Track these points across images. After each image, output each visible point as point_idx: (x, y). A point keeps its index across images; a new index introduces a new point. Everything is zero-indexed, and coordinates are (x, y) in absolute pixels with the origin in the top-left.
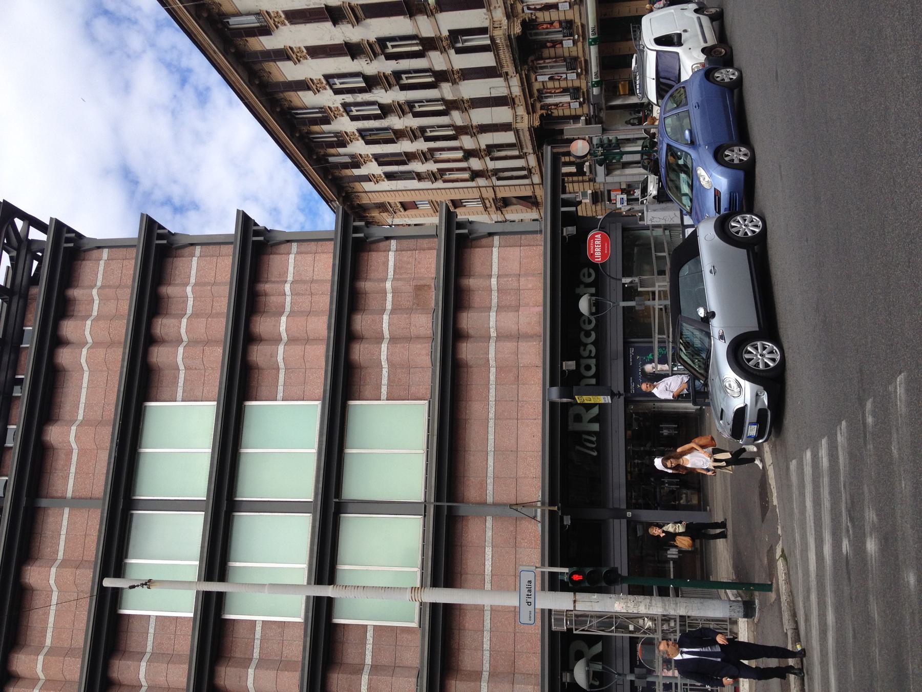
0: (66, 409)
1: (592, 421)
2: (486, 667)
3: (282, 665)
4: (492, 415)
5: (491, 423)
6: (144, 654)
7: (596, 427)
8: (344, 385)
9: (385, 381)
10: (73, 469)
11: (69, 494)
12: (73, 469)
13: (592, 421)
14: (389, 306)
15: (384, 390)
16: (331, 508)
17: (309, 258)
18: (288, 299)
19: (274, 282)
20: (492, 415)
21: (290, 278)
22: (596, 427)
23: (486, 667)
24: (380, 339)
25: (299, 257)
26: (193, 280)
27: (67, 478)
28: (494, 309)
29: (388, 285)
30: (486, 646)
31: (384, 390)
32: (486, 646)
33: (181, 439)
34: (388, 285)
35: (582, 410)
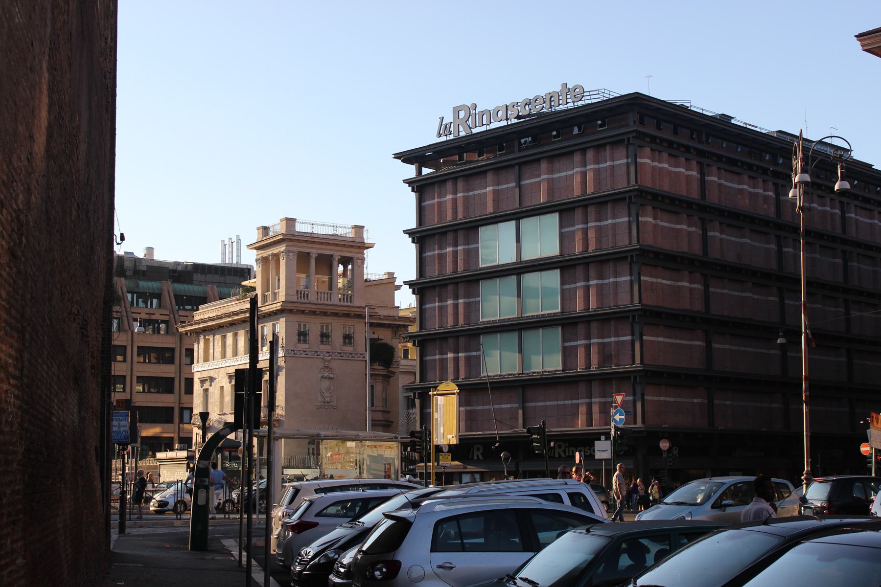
0: (557, 165)
1: (559, 454)
2: (475, 408)
3: (467, 316)
4: (560, 403)
5: (555, 403)
6: (468, 244)
7: (557, 456)
8: (567, 323)
9: (573, 344)
10: (533, 180)
11: (523, 183)
12: (533, 180)
13: (559, 454)
14: (606, 340)
15: (568, 344)
16: (520, 327)
17: (628, 289)
18: (607, 281)
19: (615, 271)
20: (560, 403)
21: (619, 279)
22: (557, 456)
23: (475, 408)
24: (588, 338)
25: (628, 284)
26: (617, 221)
27: (529, 178)
28: (603, 400)
29: (613, 339)
30: (479, 408)
31: (568, 344)
32: (479, 408)
33: (543, 238)
34: (613, 339)
35: (563, 448)
